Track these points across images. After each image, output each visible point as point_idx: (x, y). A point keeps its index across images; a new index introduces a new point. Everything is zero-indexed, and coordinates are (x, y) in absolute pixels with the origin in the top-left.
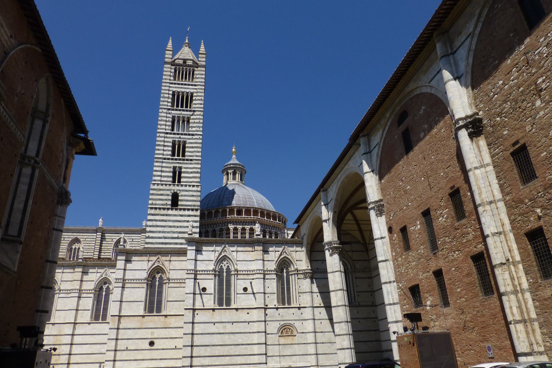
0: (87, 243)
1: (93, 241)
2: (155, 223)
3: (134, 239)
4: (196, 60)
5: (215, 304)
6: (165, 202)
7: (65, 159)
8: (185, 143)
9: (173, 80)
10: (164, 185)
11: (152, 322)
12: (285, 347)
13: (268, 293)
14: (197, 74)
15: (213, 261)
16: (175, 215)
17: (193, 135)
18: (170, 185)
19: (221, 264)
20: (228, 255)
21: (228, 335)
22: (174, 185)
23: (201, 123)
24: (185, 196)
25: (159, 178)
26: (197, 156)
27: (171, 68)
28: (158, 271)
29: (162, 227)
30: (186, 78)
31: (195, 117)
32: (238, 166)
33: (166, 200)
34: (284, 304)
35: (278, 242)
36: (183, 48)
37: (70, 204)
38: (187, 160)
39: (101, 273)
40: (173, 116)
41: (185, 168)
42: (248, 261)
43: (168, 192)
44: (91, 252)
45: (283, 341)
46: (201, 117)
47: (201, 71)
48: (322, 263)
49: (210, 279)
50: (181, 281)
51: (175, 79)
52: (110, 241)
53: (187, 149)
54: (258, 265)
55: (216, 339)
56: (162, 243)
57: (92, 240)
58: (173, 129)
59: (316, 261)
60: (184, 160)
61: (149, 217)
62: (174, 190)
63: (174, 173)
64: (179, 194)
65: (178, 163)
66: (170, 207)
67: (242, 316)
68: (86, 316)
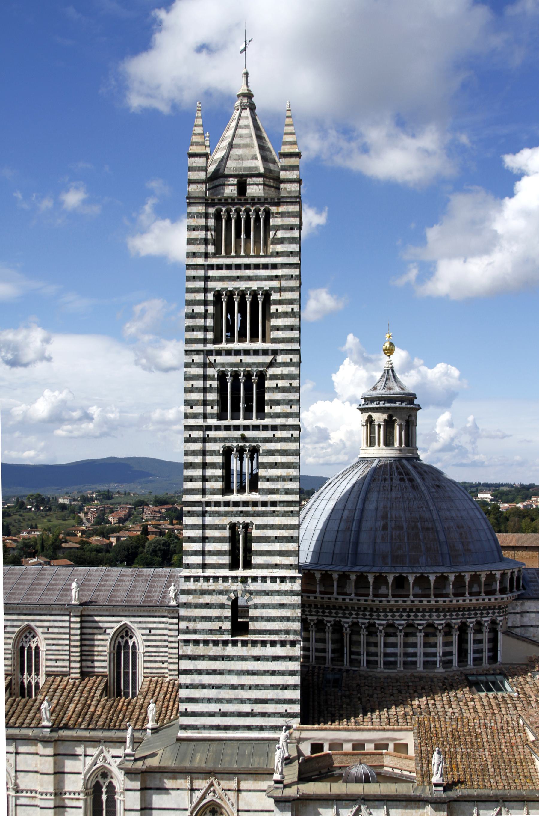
1: (65, 633)
2: (197, 679)
3: (154, 628)
10: (211, 580)
14: (278, 228)
16: (243, 659)
24: (264, 606)
26: (288, 492)
27: (206, 216)
28: (213, 808)
29: (213, 687)
39: (92, 756)
40: (219, 371)
41: (259, 527)
43: (223, 599)
44: (63, 660)
46: (293, 369)
56: (218, 728)
57: (62, 630)
58: (221, 416)
62: (235, 592)
63: (233, 539)
65: (242, 512)
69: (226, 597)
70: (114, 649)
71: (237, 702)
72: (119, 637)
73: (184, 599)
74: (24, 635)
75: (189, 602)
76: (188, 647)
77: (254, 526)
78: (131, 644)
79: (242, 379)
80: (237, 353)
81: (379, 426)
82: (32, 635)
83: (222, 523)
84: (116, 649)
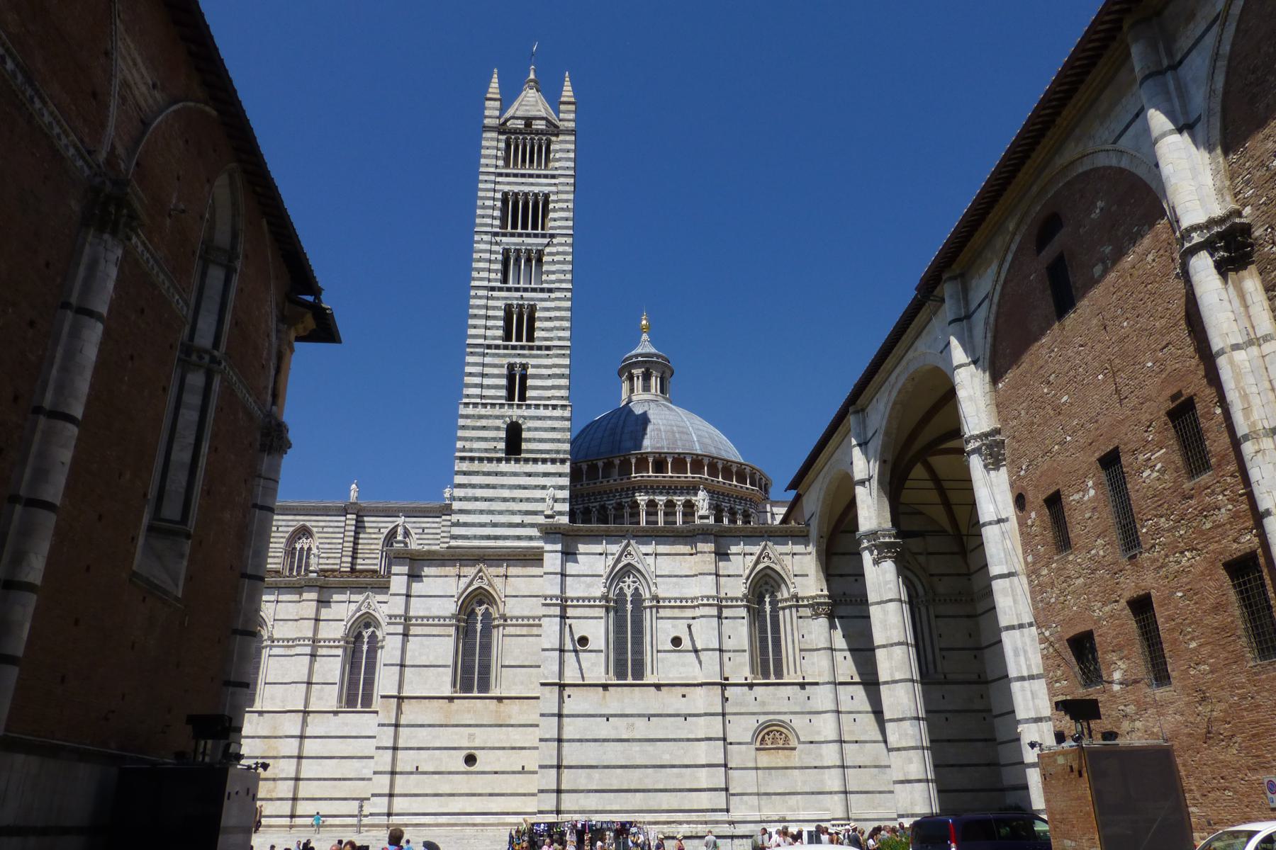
0: (326, 538)
1: (339, 533)
2: (470, 492)
3: (427, 528)
4: (553, 117)
5: (607, 673)
6: (491, 445)
7: (274, 352)
8: (533, 309)
9: (503, 168)
10: (489, 407)
11: (469, 712)
12: (770, 774)
13: (730, 651)
14: (557, 151)
15: (601, 576)
16: (515, 474)
17: (550, 290)
18: (502, 405)
19: (621, 584)
20: (636, 564)
21: (639, 743)
22: (511, 406)
23: (568, 263)
24: (536, 429)
25: (477, 391)
26: (560, 339)
27: (498, 140)
29: (486, 500)
30: (532, 161)
31: (554, 250)
32: (655, 359)
33: (494, 439)
34: (766, 674)
35: (751, 532)
36: (524, 93)
37: (289, 451)
38: (539, 348)
40: (504, 249)
41: (533, 366)
42: (681, 576)
43: (499, 423)
44: (335, 558)
45: (765, 759)
46: (567, 248)
47: (566, 142)
48: (856, 580)
49: (596, 618)
50: (532, 623)
51: (507, 165)
52: (374, 533)
53: (537, 324)
54: (705, 587)
55: (613, 754)
56: (488, 538)
57: (337, 530)
58: (505, 280)
59: (841, 576)
60: (531, 348)
61: (459, 479)
62: (510, 417)
63: (511, 377)
64: (523, 427)
65: (519, 354)
66: (504, 455)
67: (671, 701)
68: (328, 697)
81: (638, 378)
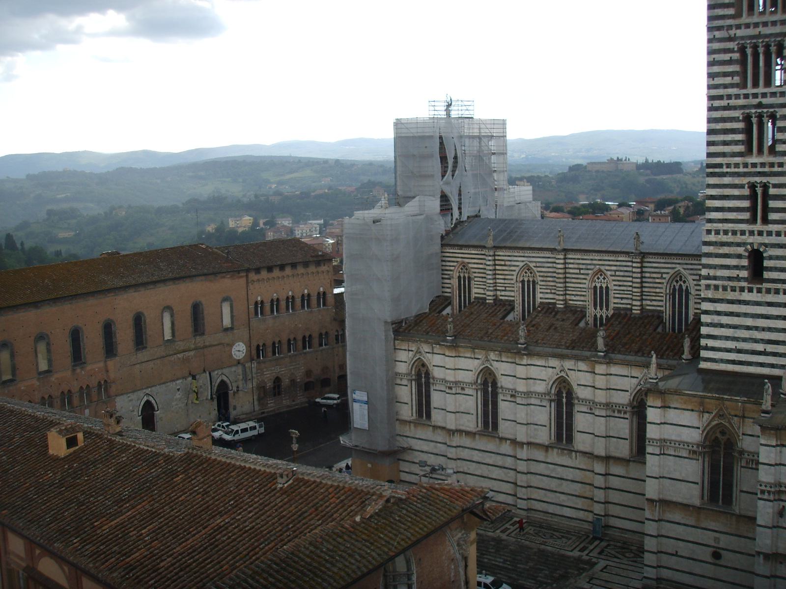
0: (618, 281)
1: (629, 277)
2: (716, 319)
6: (734, 273)
10: (730, 234)
33: (736, 267)
39: (637, 378)
40: (738, 44)
41: (775, 186)
43: (740, 250)
44: (627, 298)
56: (733, 362)
57: (626, 274)
62: (752, 244)
63: (753, 197)
64: (765, 255)
65: (759, 172)
69: (744, 248)
70: (670, 291)
71: (751, 341)
72: (674, 282)
73: (706, 249)
74: (597, 277)
75: (710, 252)
76: (708, 291)
77: (771, 185)
78: (684, 288)
79: (761, 50)
80: (756, 25)
82: (603, 277)
83: (741, 183)
84: (671, 291)
